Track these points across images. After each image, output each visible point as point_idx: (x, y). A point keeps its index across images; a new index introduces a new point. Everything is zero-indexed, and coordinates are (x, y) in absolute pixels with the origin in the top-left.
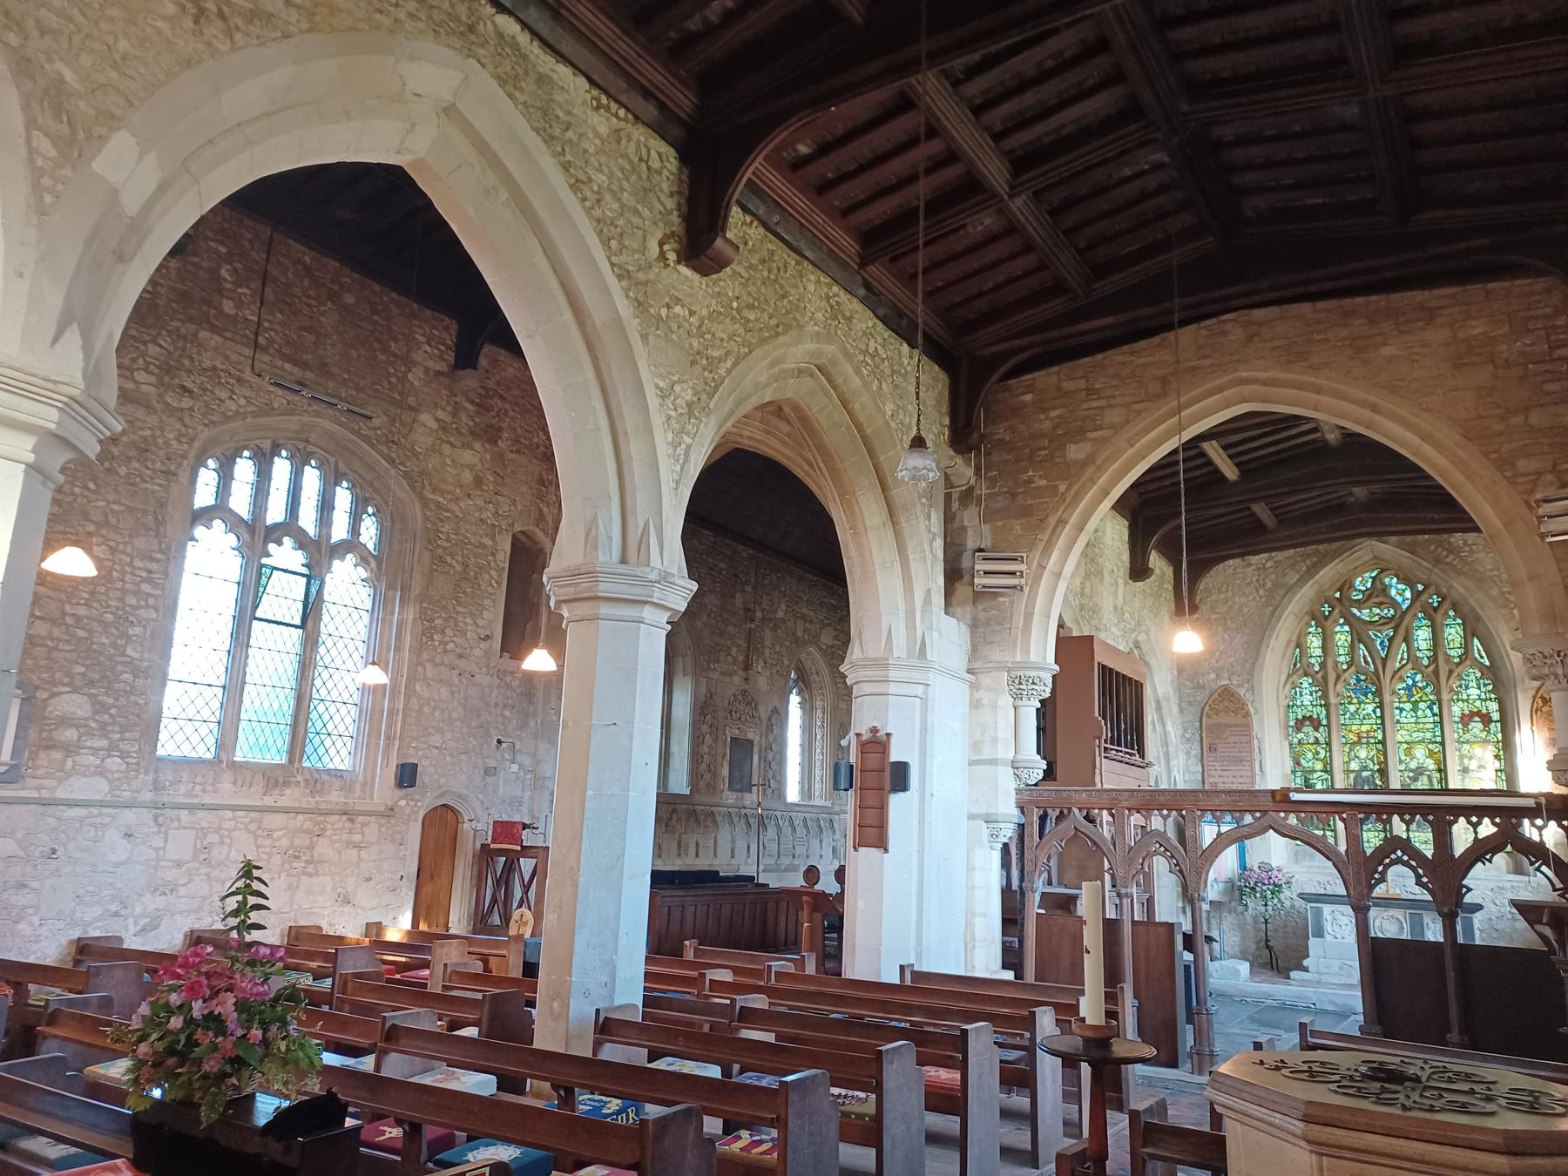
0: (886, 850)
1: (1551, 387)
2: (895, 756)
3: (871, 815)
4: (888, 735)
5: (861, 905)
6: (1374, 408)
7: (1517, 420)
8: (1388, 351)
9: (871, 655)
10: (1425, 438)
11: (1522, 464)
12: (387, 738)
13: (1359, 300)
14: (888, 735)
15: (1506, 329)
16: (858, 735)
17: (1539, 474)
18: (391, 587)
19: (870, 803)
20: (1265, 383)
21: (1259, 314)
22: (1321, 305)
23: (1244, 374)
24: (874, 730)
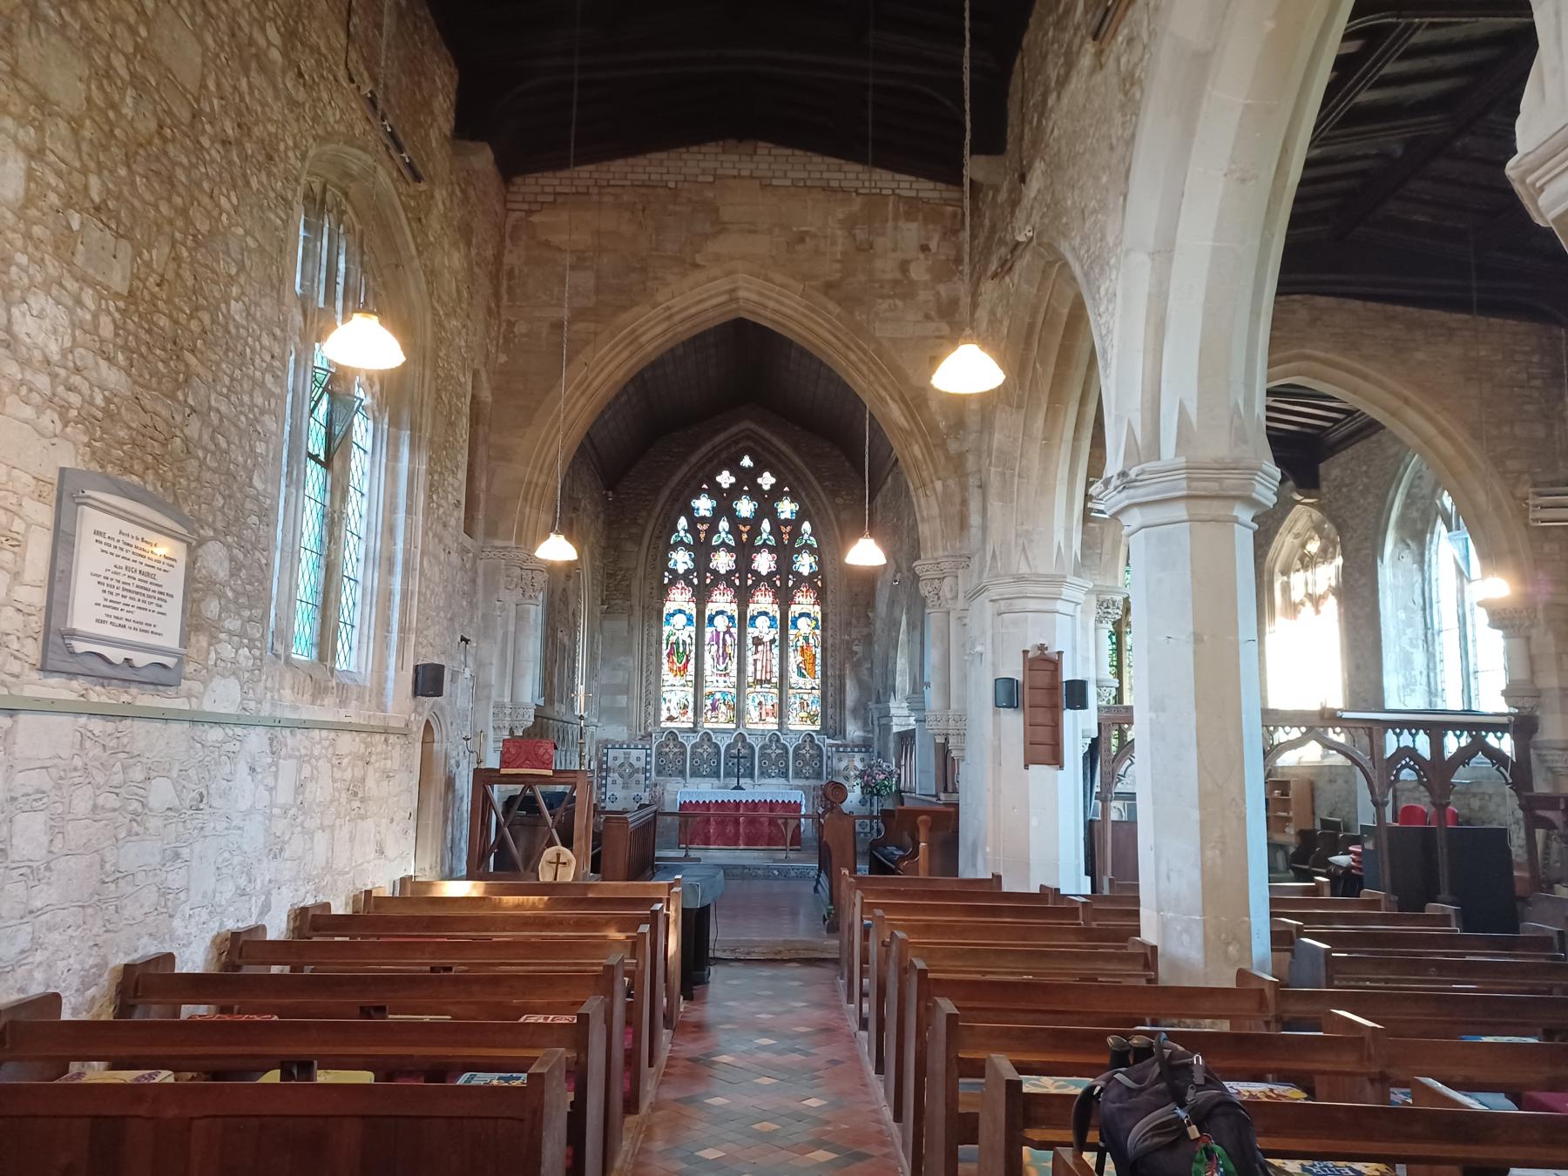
0: (1061, 767)
1: (1528, 407)
2: (1067, 676)
3: (1043, 734)
4: (1060, 653)
5: (1034, 822)
6: (1406, 401)
7: (1506, 429)
8: (1420, 356)
9: (1041, 571)
10: (1443, 432)
11: (1512, 464)
12: (402, 629)
13: (1399, 308)
14: (1060, 653)
15: (1500, 357)
16: (1026, 652)
17: (1521, 473)
18: (395, 422)
19: (1040, 720)
20: (1324, 362)
21: (1322, 301)
22: (1371, 305)
23: (1308, 351)
24: (1042, 648)
